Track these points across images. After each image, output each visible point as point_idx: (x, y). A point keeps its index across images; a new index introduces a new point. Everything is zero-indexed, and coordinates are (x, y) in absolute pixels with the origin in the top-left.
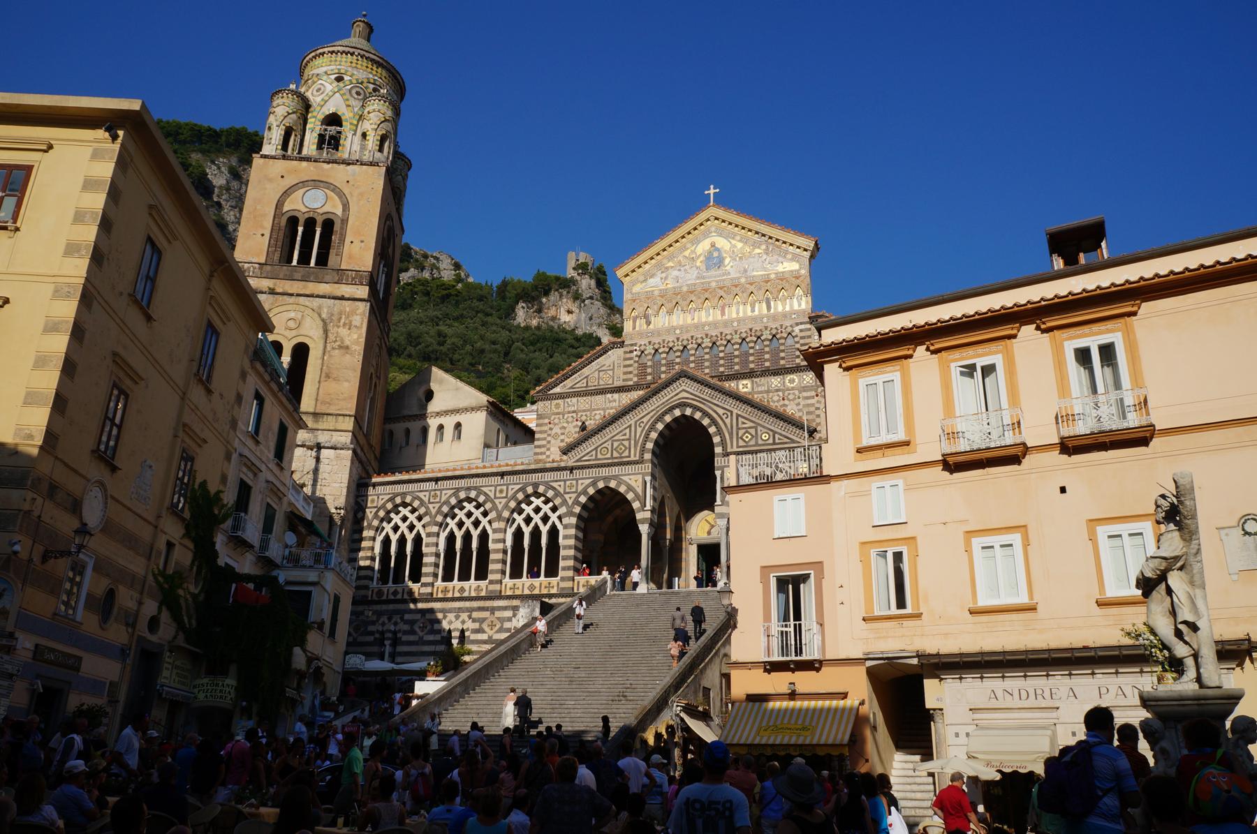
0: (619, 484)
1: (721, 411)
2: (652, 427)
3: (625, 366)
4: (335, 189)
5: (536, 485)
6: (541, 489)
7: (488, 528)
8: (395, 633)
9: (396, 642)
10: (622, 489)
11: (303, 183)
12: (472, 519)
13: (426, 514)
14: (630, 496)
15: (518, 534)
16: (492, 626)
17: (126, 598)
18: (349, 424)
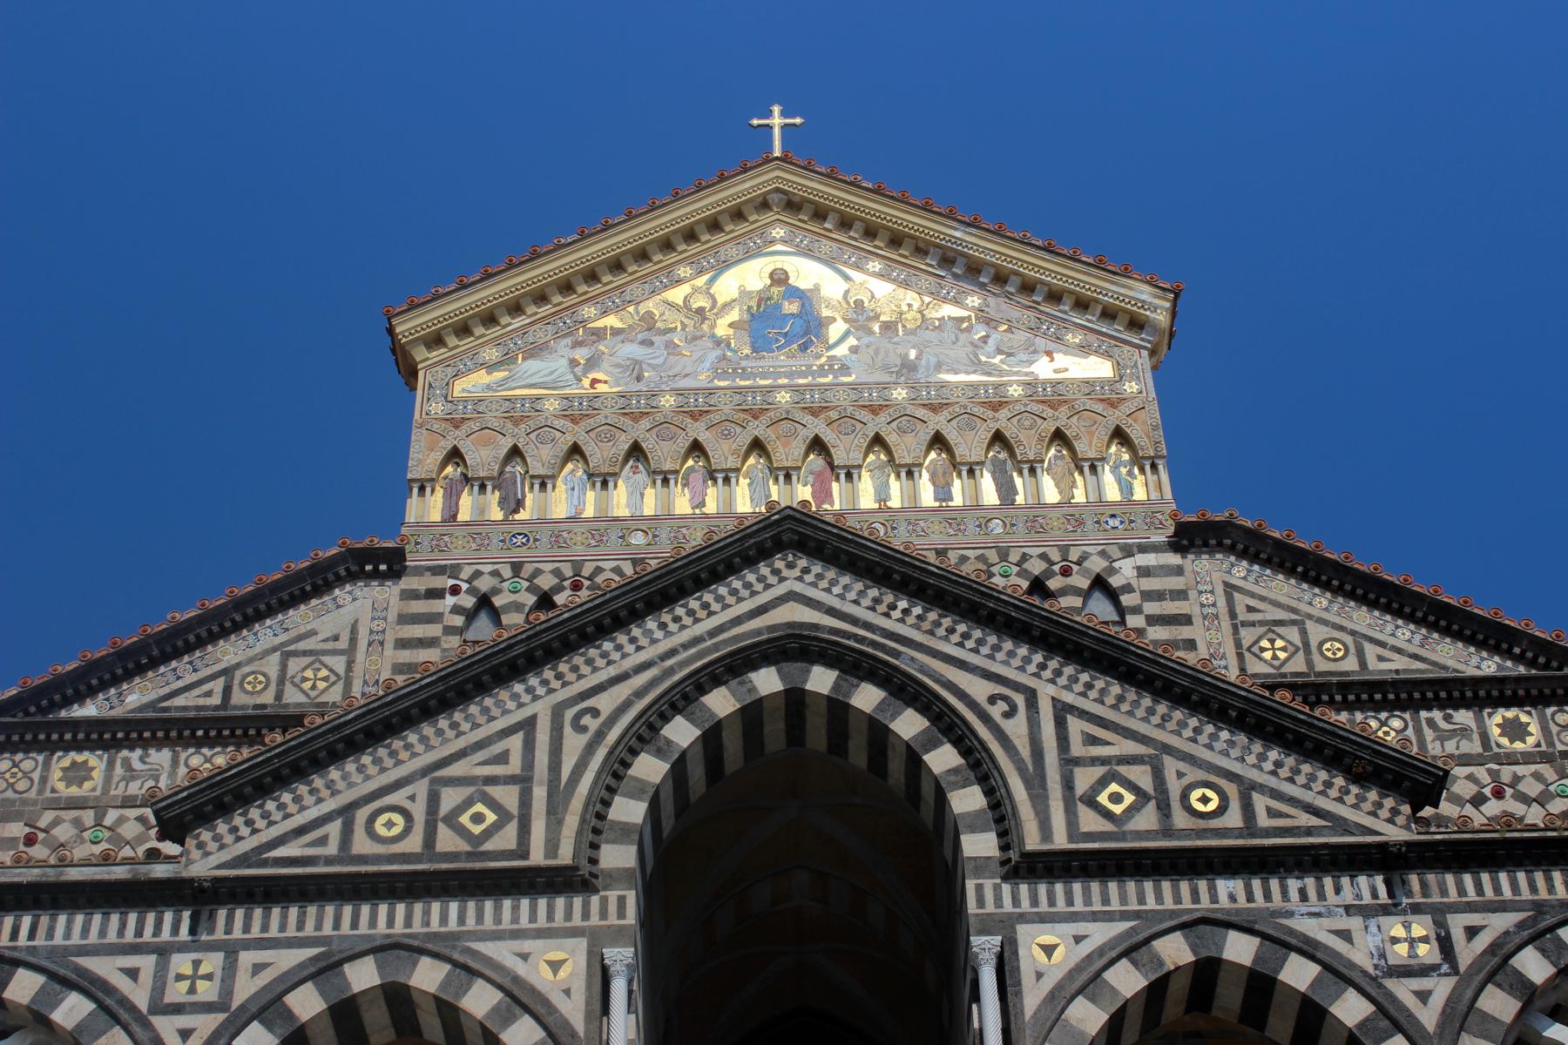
1: (980, 689)
2: (645, 734)
3: (402, 644)
10: (479, 1001)
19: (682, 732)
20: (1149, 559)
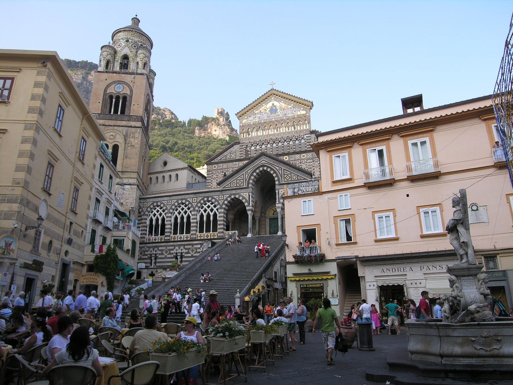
0: (240, 196)
1: (278, 168)
2: (252, 175)
4: (127, 84)
5: (208, 197)
6: (210, 199)
7: (190, 214)
8: (156, 254)
9: (156, 258)
10: (241, 198)
11: (114, 82)
12: (184, 211)
13: (166, 209)
14: (244, 201)
15: (202, 216)
16: (193, 251)
17: (56, 244)
18: (135, 175)
19: (255, 174)
20: (307, 135)
